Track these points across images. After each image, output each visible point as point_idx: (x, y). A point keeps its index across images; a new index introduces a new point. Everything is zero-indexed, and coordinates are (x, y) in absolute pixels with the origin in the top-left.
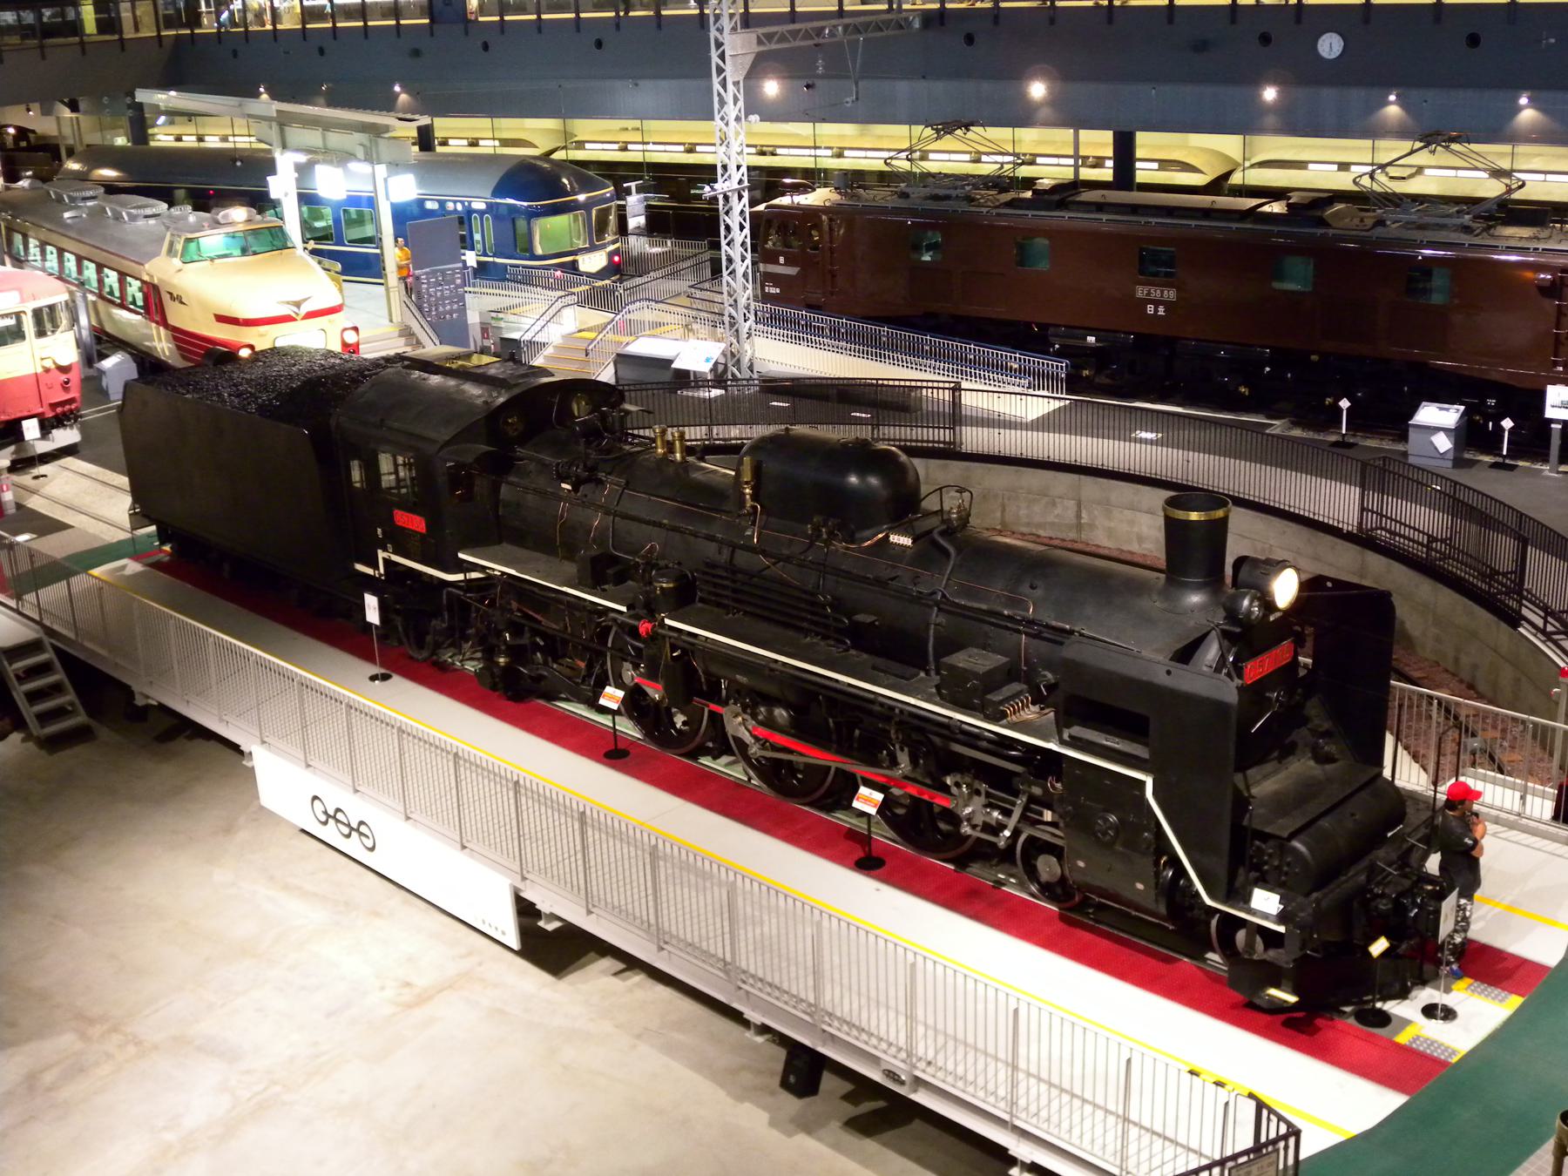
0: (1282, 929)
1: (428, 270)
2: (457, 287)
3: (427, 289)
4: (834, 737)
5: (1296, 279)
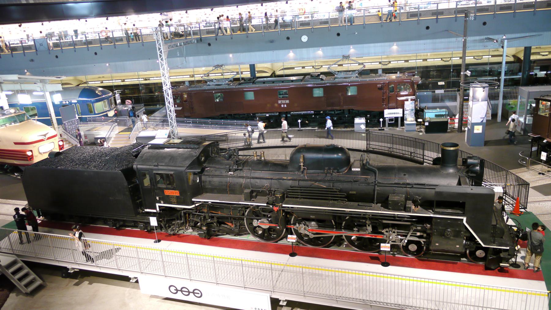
1: (67, 121)
2: (76, 125)
3: (68, 127)
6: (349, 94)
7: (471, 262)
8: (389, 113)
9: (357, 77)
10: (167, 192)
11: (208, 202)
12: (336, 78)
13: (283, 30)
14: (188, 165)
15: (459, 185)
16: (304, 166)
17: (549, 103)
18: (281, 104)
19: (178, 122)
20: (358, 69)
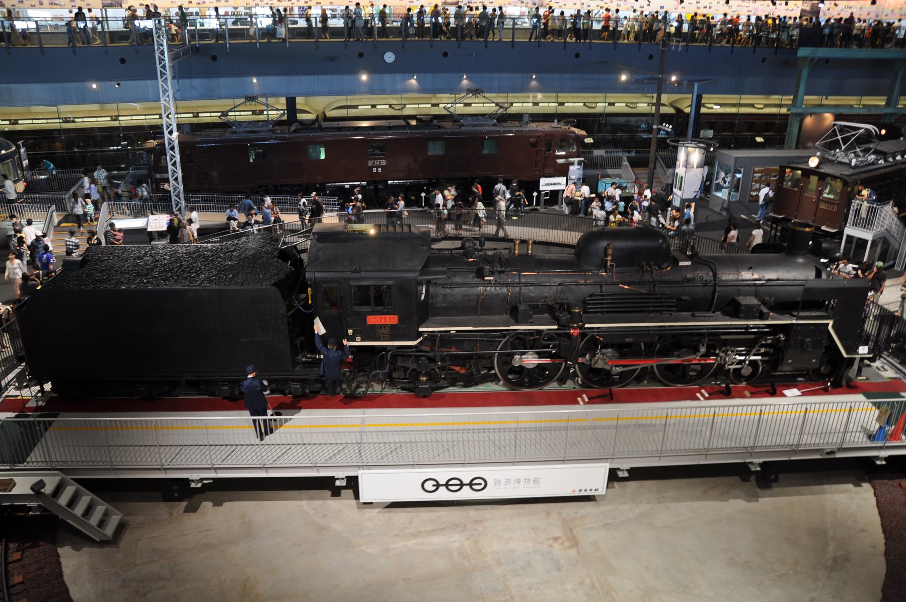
0: (871, 356)
4: (644, 353)
5: (435, 150)
8: (546, 184)
9: (494, 125)
10: (372, 320)
11: (450, 331)
12: (462, 125)
14: (421, 268)
16: (611, 261)
17: (800, 172)
19: (187, 200)
20: (490, 113)
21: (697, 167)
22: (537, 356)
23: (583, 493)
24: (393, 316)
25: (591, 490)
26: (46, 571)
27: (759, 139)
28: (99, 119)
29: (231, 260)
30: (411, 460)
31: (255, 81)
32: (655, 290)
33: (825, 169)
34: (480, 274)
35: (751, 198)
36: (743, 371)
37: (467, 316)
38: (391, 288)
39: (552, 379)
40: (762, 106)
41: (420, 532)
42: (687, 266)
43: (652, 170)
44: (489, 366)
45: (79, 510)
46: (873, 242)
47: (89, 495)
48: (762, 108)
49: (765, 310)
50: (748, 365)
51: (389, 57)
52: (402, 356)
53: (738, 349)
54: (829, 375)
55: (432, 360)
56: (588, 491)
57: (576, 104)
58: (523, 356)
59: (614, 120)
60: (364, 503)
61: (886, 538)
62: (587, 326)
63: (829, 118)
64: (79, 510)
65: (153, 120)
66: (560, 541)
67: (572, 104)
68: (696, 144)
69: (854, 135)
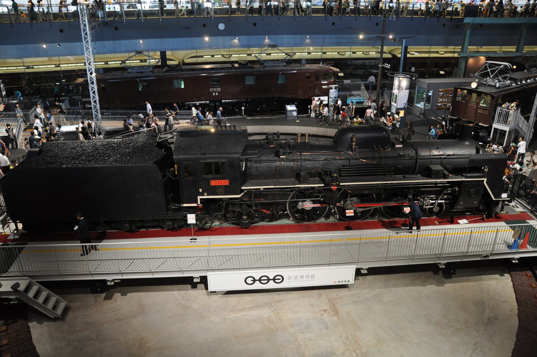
0: (509, 199)
4: (375, 200)
5: (249, 81)
6: (280, 82)
7: (475, 214)
9: (285, 66)
10: (213, 183)
11: (260, 189)
12: (266, 66)
13: (199, 16)
14: (242, 151)
15: (478, 153)
16: (355, 145)
17: (466, 91)
18: (212, 92)
19: (102, 114)
21: (405, 89)
22: (312, 203)
23: (341, 283)
24: (226, 180)
25: (345, 281)
26: (22, 336)
27: (442, 72)
28: (48, 66)
29: (128, 149)
30: (238, 265)
31: (141, 42)
32: (381, 162)
33: (481, 89)
34: (277, 155)
35: (437, 107)
36: (434, 210)
37: (270, 179)
38: (224, 164)
39: (322, 216)
40: (443, 53)
41: (244, 308)
42: (400, 148)
43: (379, 92)
44: (284, 209)
45: (41, 300)
46: (510, 132)
47: (47, 291)
48: (443, 54)
49: (447, 173)
50: (437, 206)
51: (221, 27)
52: (231, 204)
53: (431, 196)
54: (484, 211)
55: (250, 206)
56: (344, 282)
57: (333, 53)
58: (304, 203)
59: (356, 62)
60: (211, 292)
61: (518, 306)
62: (341, 184)
63: (483, 59)
64: (41, 300)
65: (80, 66)
66: (328, 312)
67: (331, 53)
68: (404, 75)
69: (497, 69)
